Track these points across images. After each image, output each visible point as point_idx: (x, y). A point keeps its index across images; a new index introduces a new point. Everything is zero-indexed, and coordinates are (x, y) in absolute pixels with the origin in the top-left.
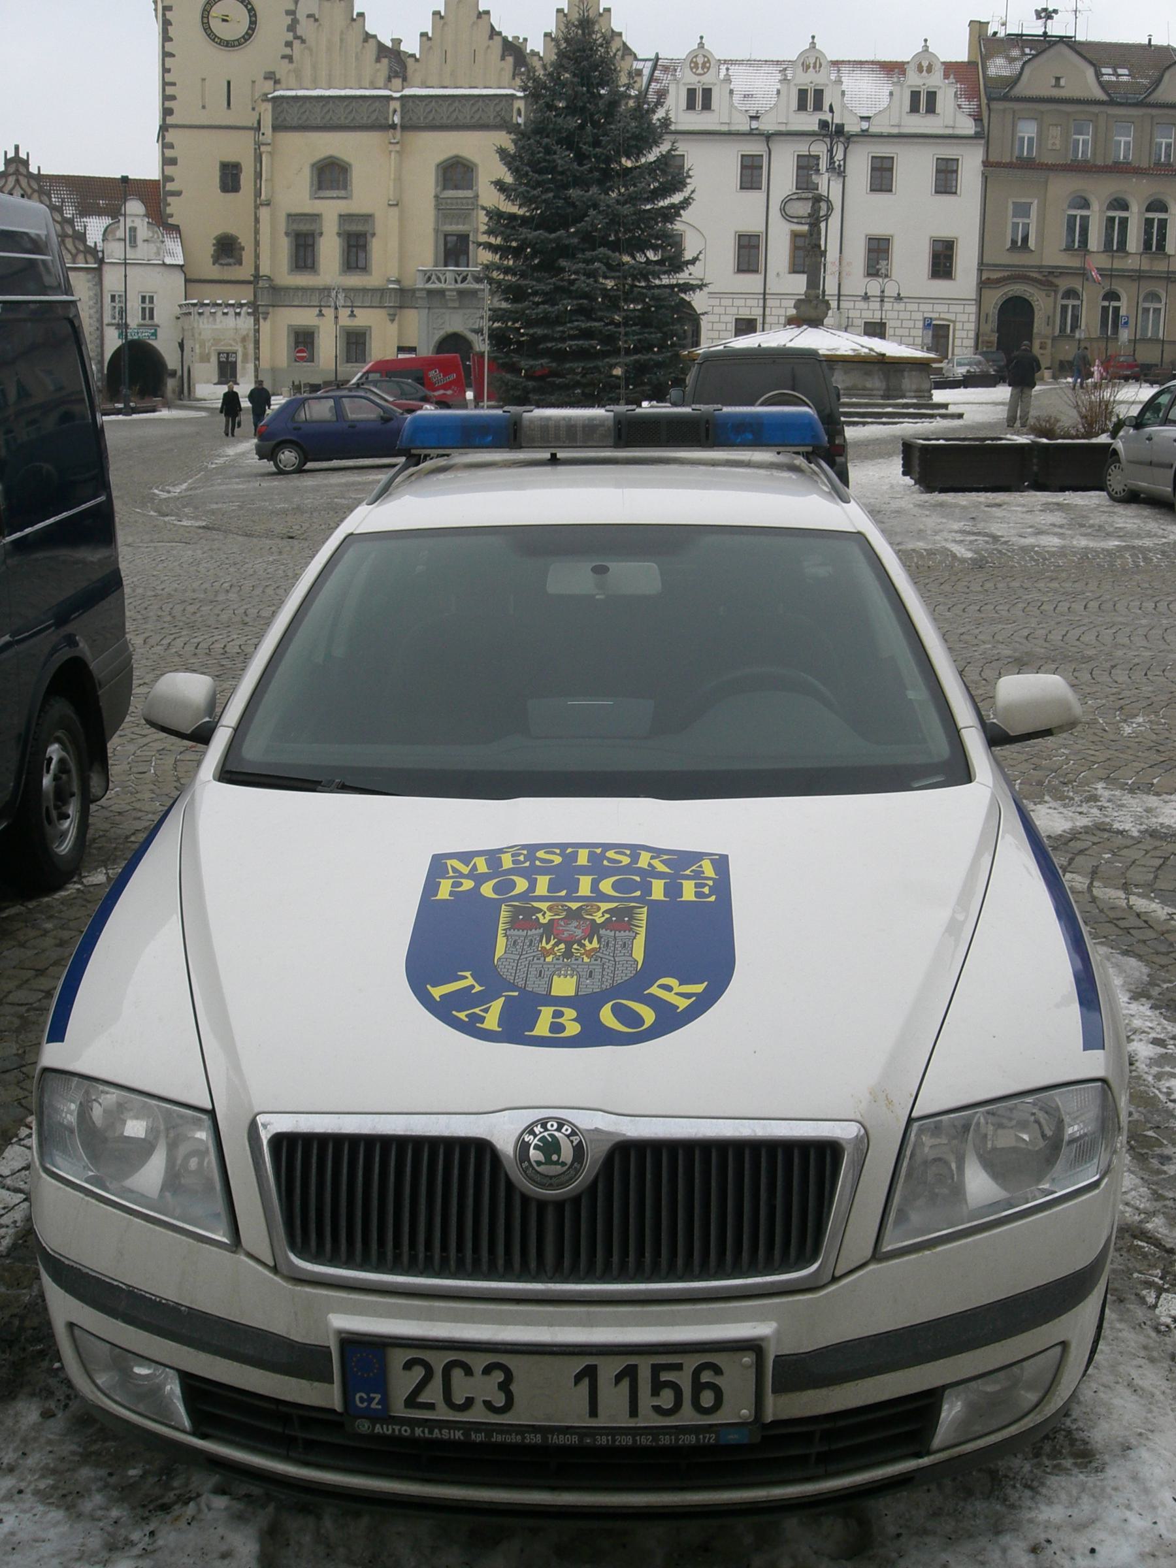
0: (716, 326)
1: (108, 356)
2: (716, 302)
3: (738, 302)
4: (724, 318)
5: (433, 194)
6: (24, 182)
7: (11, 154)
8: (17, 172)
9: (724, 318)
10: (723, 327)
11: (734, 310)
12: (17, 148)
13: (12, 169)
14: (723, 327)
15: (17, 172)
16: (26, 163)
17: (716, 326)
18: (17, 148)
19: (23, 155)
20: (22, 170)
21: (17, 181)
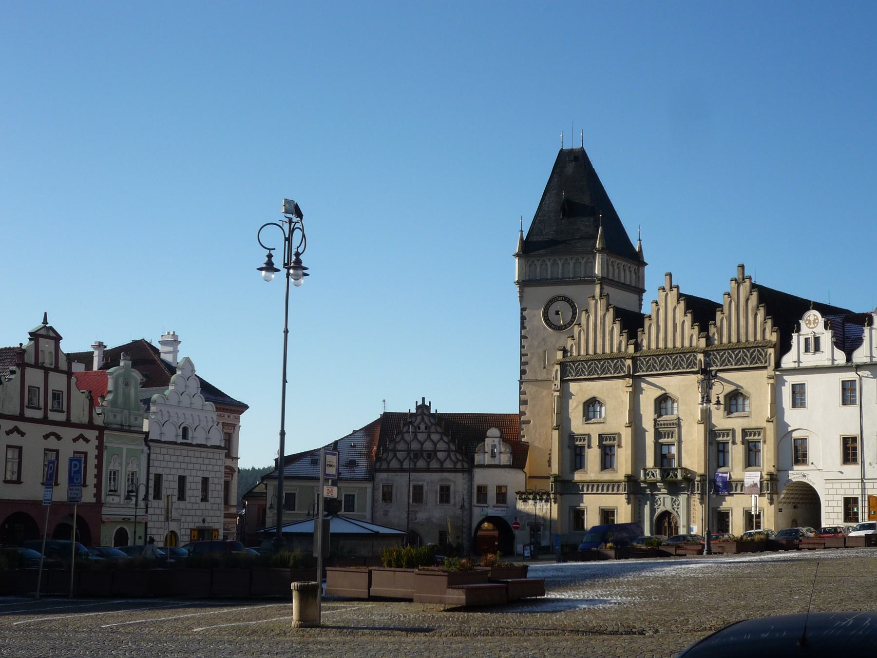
0: (831, 504)
1: (474, 525)
2: (829, 486)
3: (844, 486)
4: (836, 498)
5: (653, 418)
6: (426, 418)
7: (420, 403)
8: (423, 414)
9: (836, 498)
10: (835, 504)
11: (842, 492)
12: (423, 399)
13: (420, 411)
14: (835, 504)
15: (423, 414)
16: (428, 408)
17: (831, 504)
18: (423, 399)
19: (427, 403)
20: (426, 412)
21: (423, 419)
